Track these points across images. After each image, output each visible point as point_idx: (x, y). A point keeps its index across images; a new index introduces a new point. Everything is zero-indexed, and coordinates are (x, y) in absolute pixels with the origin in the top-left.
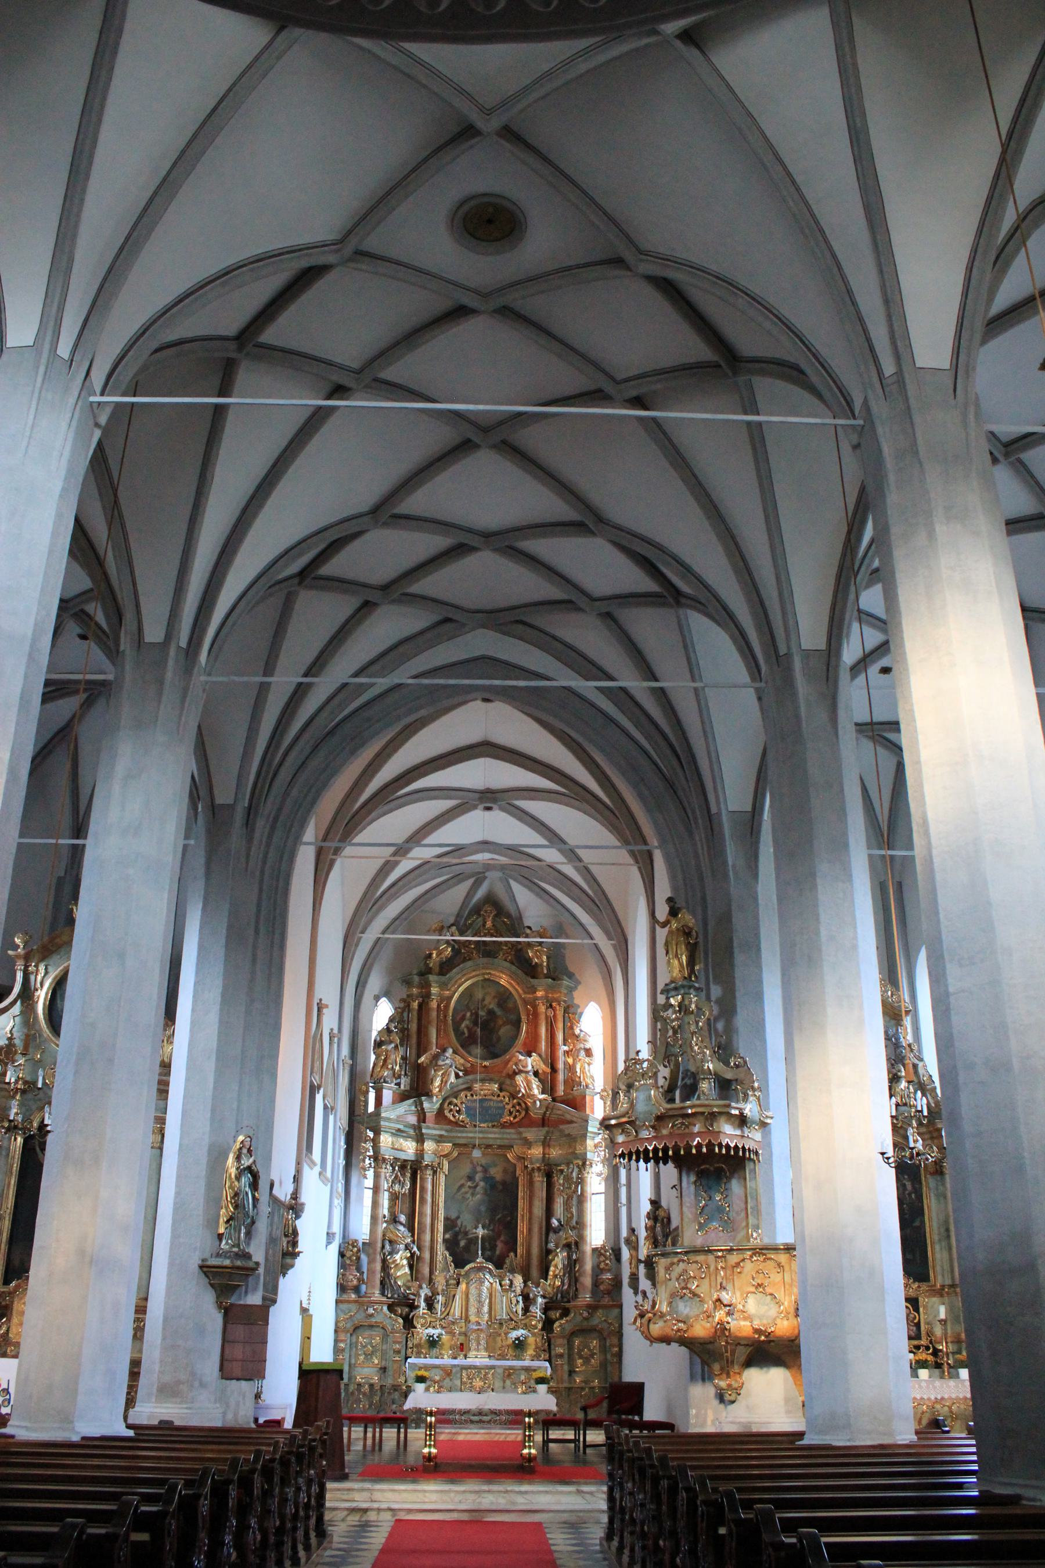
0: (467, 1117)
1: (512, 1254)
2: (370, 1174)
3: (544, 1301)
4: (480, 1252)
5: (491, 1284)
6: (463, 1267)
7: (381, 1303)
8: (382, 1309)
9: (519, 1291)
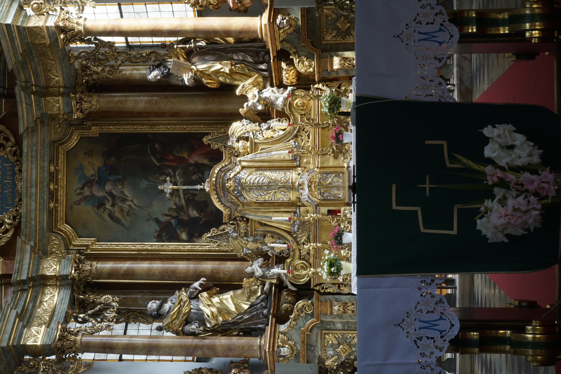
0: (6, 211)
1: (205, 140)
2: (87, 356)
3: (269, 88)
4: (199, 187)
5: (243, 168)
6: (221, 213)
7: (274, 335)
8: (284, 333)
9: (254, 126)
